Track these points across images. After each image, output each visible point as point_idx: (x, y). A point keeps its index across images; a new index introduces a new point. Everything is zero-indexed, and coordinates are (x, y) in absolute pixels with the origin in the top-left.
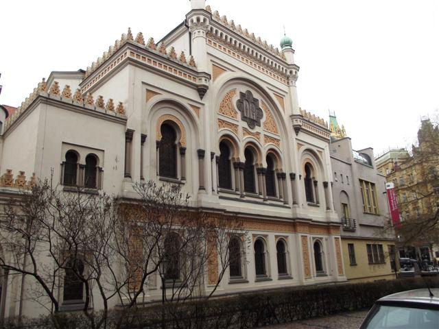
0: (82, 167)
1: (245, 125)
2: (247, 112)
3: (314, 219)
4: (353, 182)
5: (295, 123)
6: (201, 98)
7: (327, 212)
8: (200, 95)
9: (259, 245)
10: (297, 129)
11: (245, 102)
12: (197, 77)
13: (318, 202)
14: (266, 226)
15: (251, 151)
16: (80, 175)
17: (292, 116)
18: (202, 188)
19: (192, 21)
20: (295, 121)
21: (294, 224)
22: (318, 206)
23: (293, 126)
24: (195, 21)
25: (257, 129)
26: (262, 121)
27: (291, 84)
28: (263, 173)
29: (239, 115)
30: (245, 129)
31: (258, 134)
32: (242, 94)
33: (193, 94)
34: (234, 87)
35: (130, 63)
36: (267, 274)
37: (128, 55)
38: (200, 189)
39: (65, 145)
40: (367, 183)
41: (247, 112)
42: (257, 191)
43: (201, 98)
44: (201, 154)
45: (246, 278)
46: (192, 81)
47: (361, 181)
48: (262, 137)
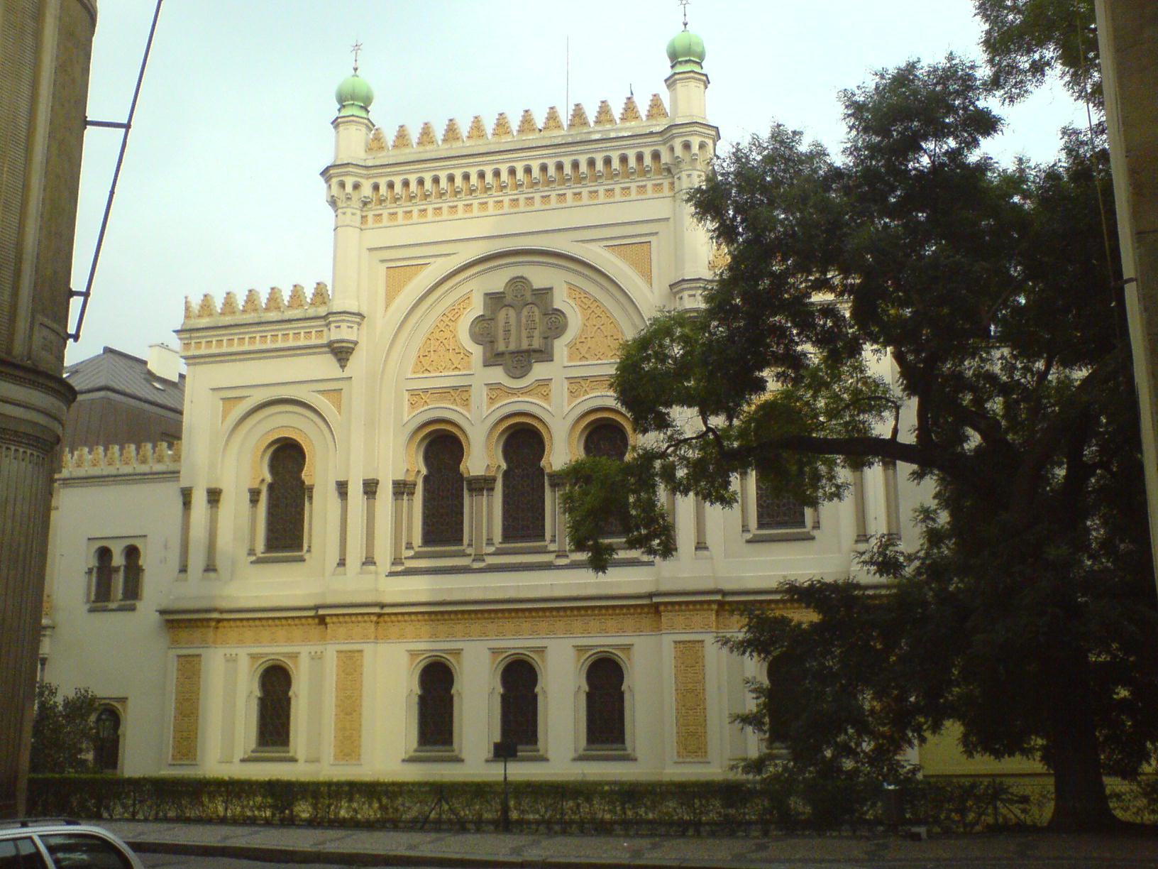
0: (117, 569)
1: (497, 375)
2: (507, 339)
3: (727, 587)
6: (343, 367)
8: (339, 360)
9: (519, 679)
11: (502, 316)
13: (817, 525)
14: (543, 625)
15: (523, 439)
16: (119, 581)
18: (342, 563)
21: (653, 608)
22: (813, 538)
25: (539, 371)
26: (560, 347)
29: (477, 351)
30: (494, 387)
31: (545, 383)
32: (495, 300)
33: (325, 366)
34: (464, 289)
36: (540, 744)
41: (507, 339)
42: (548, 536)
43: (343, 367)
44: (342, 488)
45: (461, 751)
46: (314, 341)
48: (560, 389)
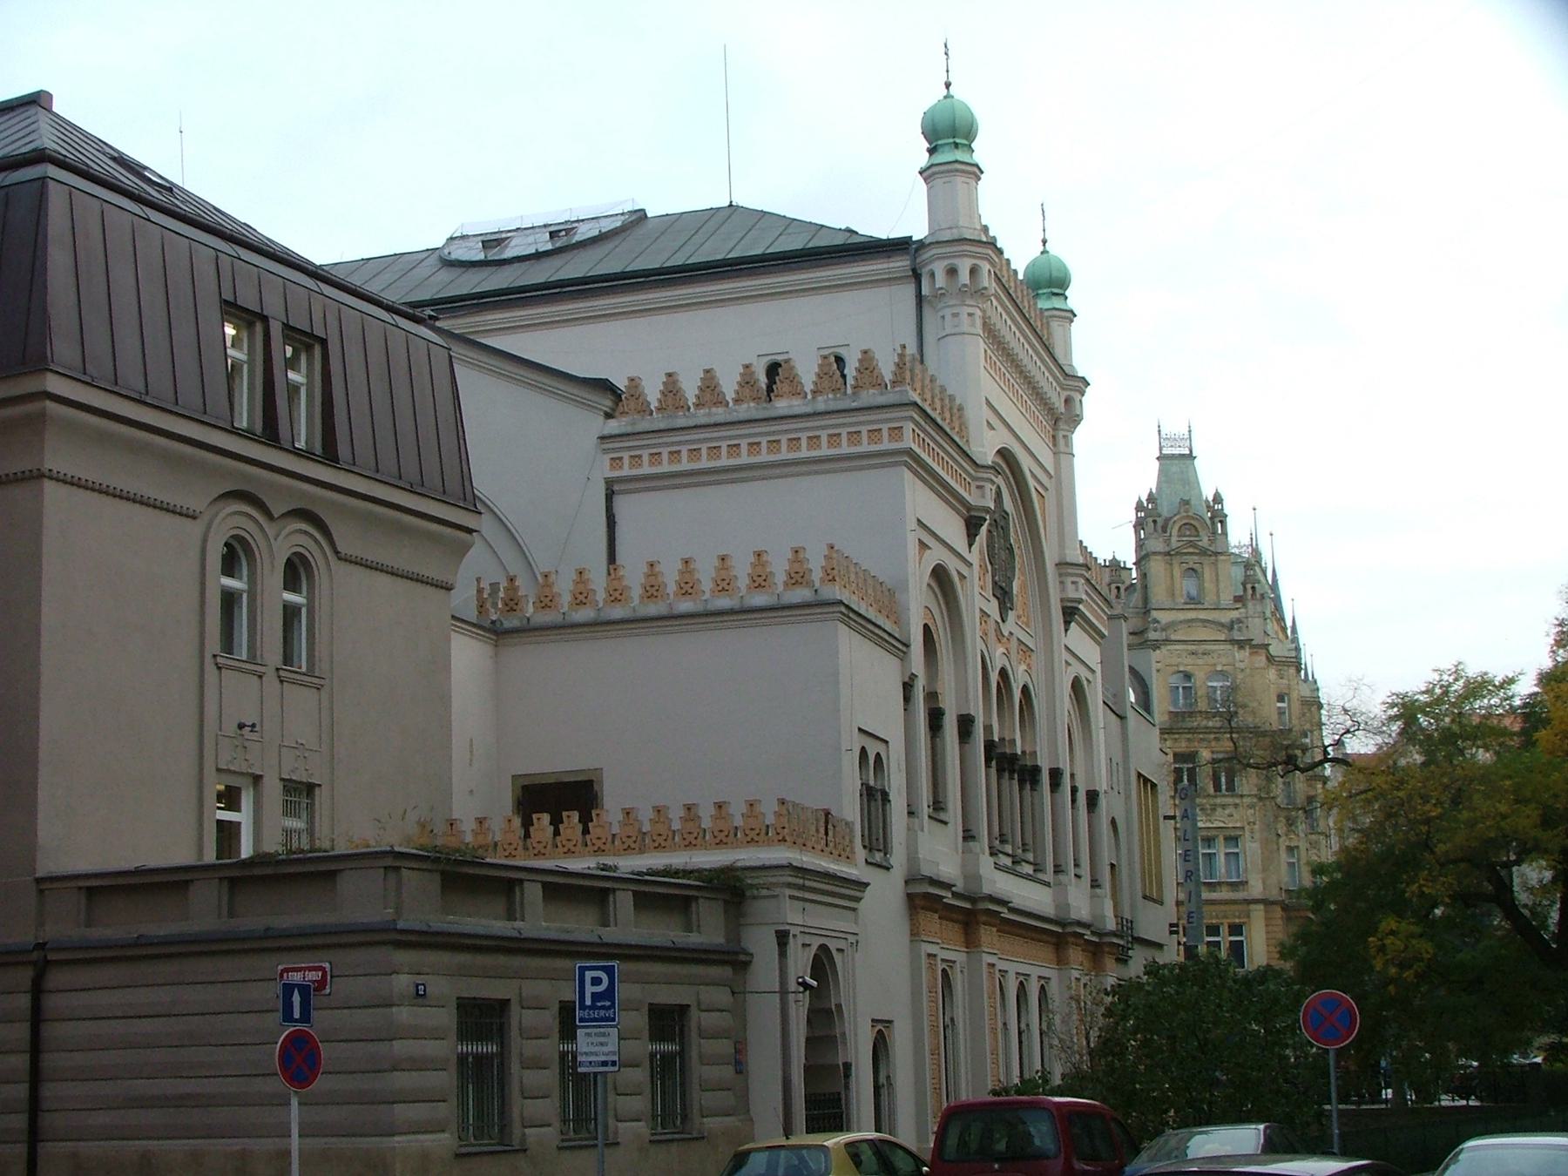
4: (1127, 783)
5: (1072, 594)
7: (1092, 897)
10: (1070, 613)
12: (975, 479)
17: (1062, 565)
19: (952, 272)
20: (1070, 587)
23: (1062, 600)
24: (964, 277)
27: (1061, 442)
28: (1012, 772)
35: (906, 464)
37: (908, 441)
38: (965, 839)
39: (863, 736)
40: (1146, 780)
47: (1140, 775)
